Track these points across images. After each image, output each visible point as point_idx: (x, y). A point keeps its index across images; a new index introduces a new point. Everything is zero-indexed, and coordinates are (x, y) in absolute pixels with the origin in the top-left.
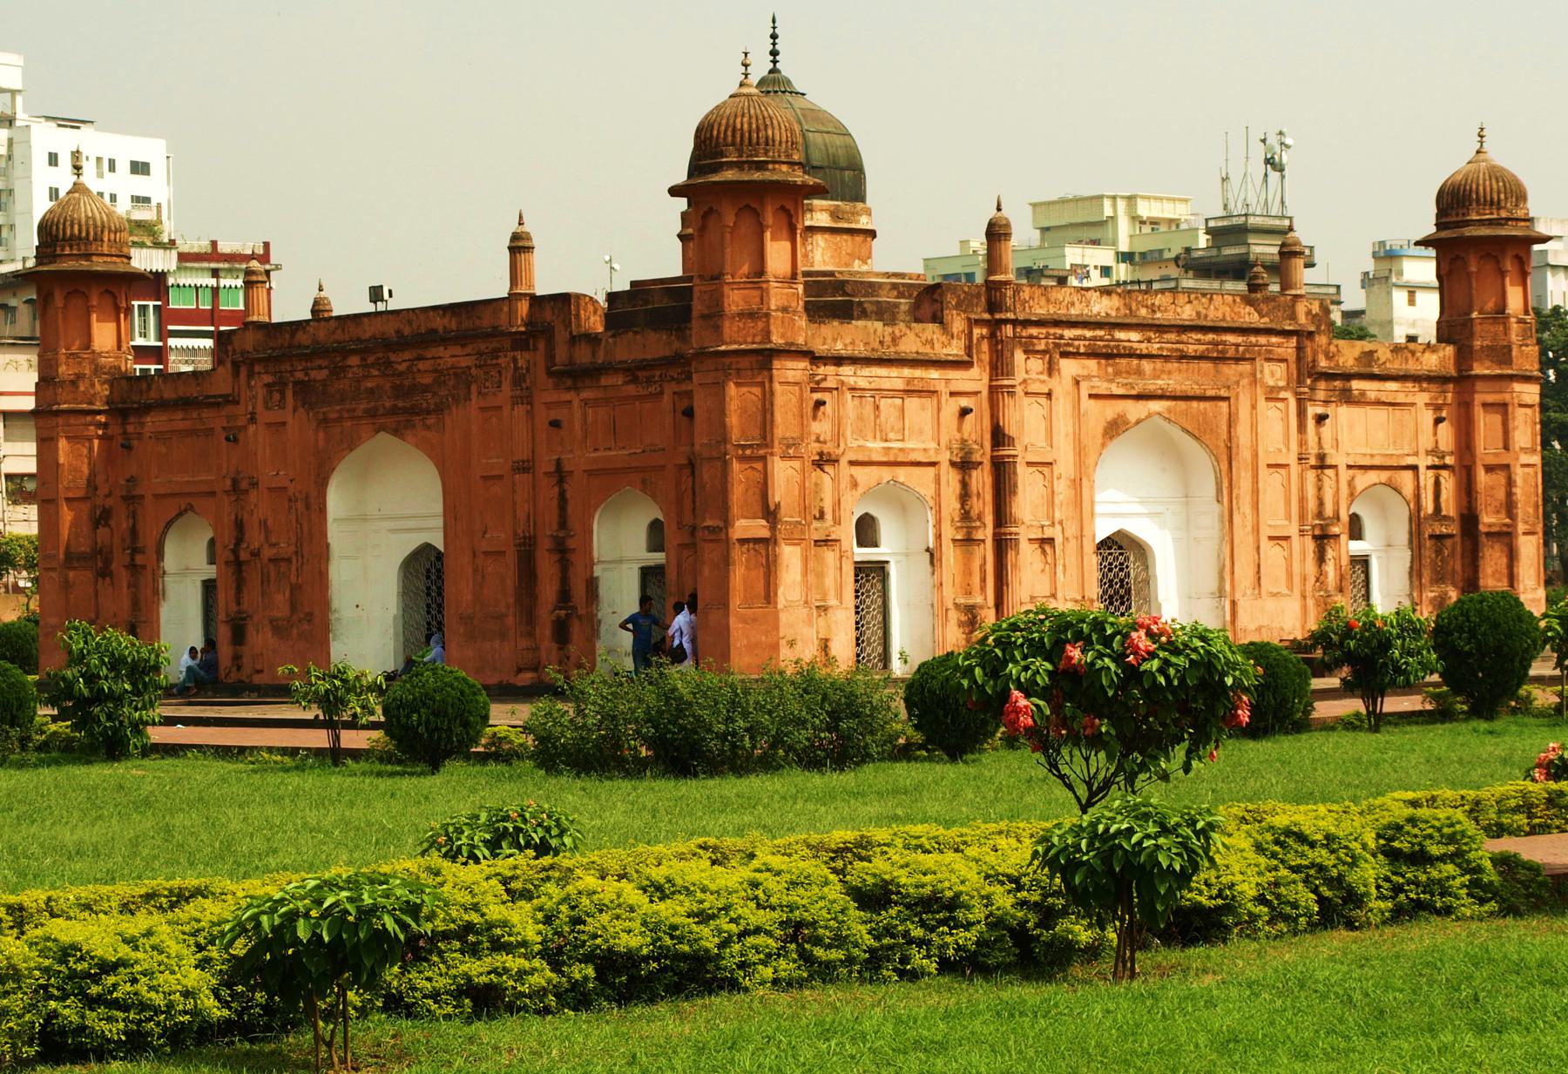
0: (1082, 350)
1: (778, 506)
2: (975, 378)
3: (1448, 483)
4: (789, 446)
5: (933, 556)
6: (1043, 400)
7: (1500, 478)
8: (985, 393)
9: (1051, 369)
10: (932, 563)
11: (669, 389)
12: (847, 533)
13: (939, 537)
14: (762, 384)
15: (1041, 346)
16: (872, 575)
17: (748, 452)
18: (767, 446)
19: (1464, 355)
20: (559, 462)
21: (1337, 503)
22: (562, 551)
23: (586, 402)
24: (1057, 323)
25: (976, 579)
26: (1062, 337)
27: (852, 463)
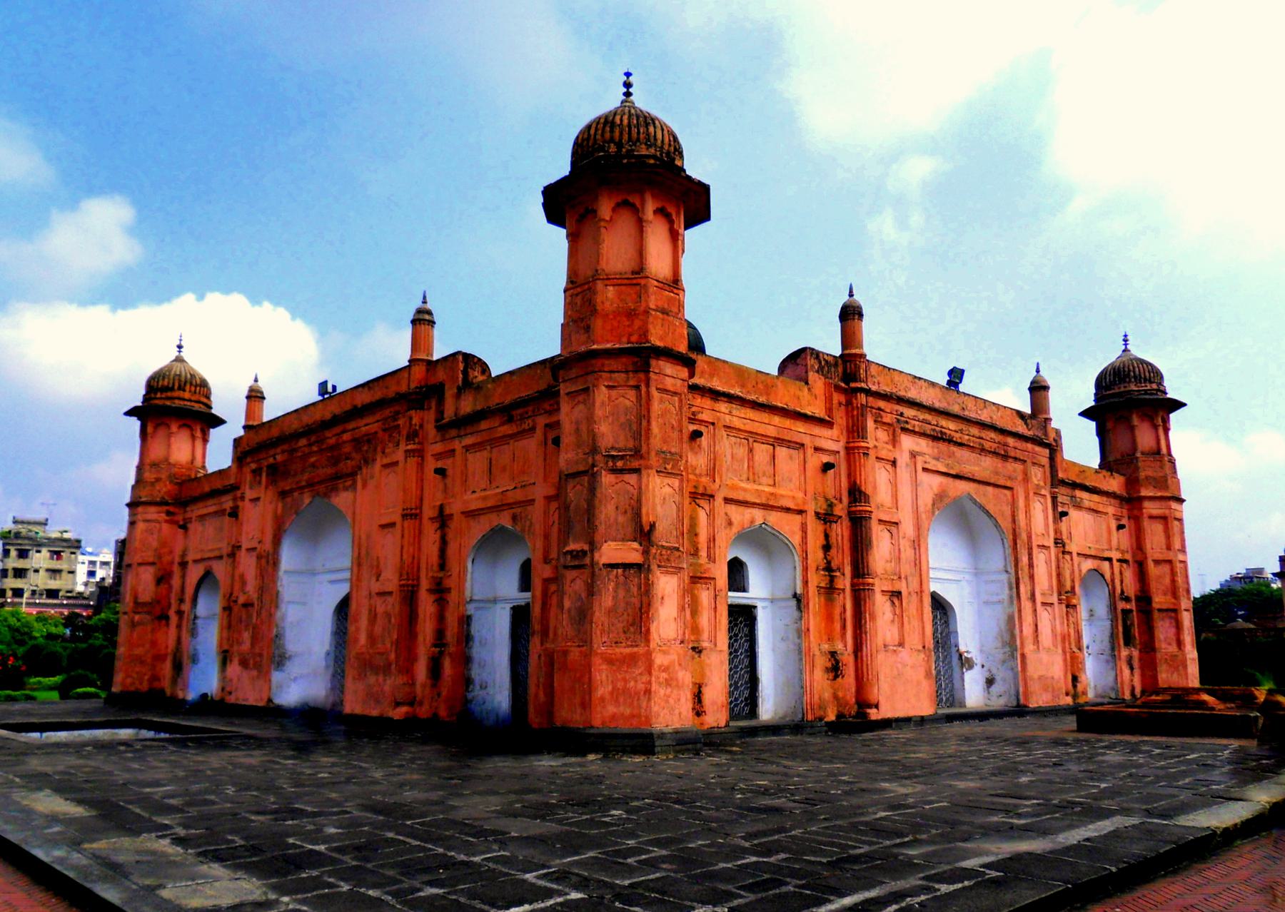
0: (917, 429)
1: (653, 526)
2: (832, 440)
3: (1129, 575)
4: (666, 461)
5: (799, 601)
6: (889, 467)
7: (1166, 568)
8: (842, 453)
9: (894, 441)
10: (799, 608)
11: (542, 421)
12: (721, 573)
13: (805, 583)
14: (637, 387)
15: (888, 418)
16: (743, 618)
17: (620, 464)
18: (642, 457)
19: (1132, 482)
20: (441, 508)
21: (1073, 581)
22: (440, 591)
23: (467, 448)
24: (901, 400)
25: (838, 626)
26: (902, 415)
27: (727, 501)
